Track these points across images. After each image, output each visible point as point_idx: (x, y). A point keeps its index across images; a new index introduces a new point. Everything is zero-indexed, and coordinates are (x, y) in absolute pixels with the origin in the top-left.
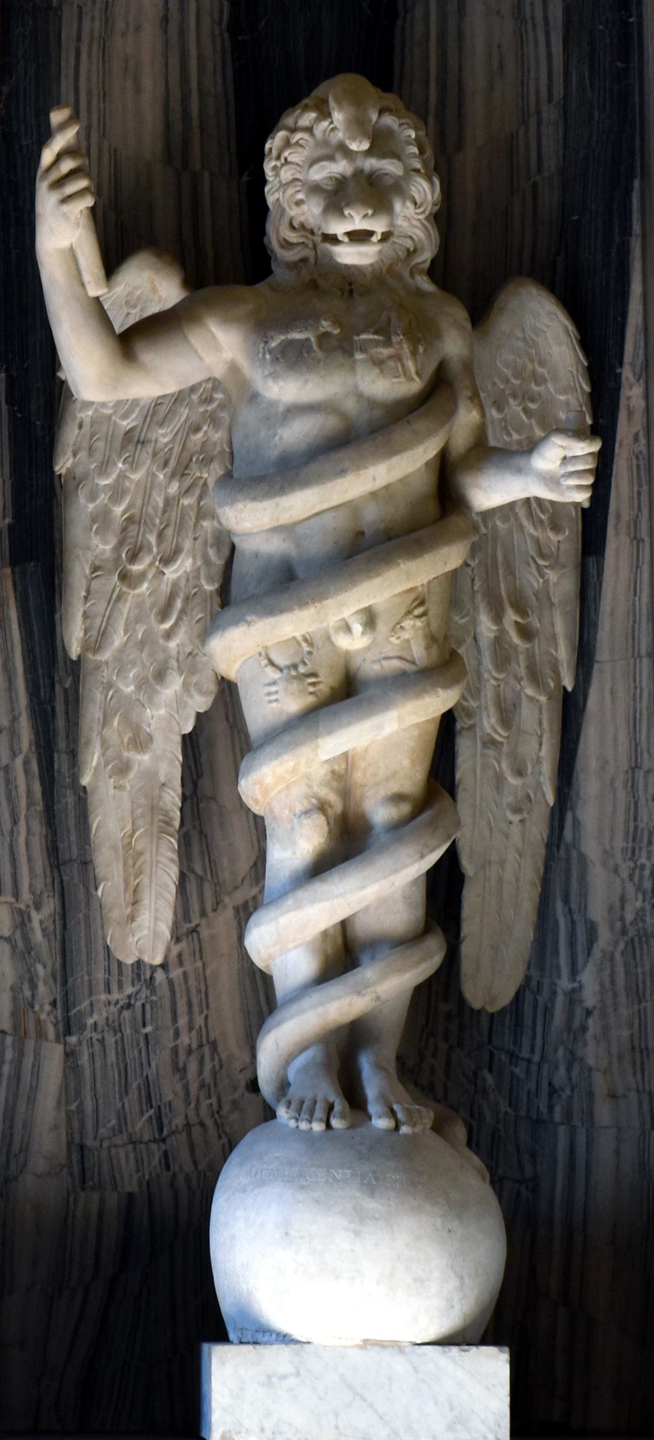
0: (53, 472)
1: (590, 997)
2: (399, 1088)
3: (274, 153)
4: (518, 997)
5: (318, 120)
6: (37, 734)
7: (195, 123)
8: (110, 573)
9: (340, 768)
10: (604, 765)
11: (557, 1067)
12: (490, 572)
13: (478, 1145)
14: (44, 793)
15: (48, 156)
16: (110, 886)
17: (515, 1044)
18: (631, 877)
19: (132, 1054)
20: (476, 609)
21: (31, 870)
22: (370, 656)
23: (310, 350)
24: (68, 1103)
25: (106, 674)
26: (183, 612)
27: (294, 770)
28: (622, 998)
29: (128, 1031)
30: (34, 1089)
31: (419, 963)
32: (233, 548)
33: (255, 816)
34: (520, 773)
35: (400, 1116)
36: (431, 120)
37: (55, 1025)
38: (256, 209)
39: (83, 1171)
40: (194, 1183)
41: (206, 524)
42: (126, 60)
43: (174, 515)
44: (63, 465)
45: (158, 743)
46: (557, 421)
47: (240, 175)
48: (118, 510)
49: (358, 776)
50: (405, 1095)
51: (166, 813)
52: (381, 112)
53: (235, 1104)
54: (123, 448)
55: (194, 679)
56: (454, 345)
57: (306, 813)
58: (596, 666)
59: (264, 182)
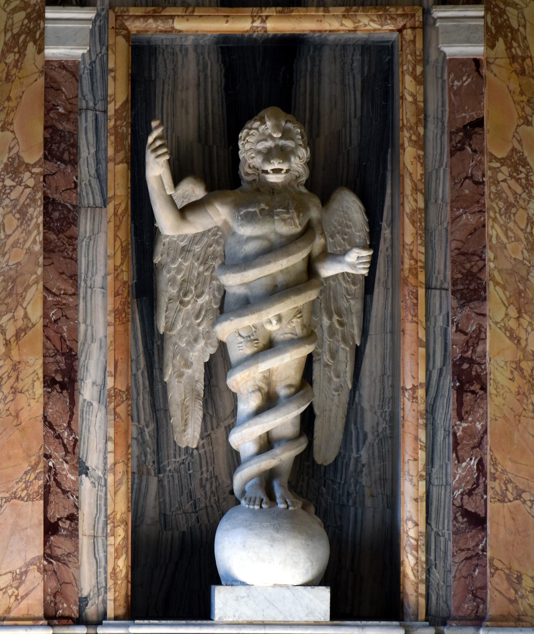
0: (153, 262)
1: (364, 459)
2: (289, 493)
3: (243, 138)
4: (336, 460)
5: (260, 125)
6: (147, 362)
7: (211, 126)
8: (176, 301)
9: (267, 375)
10: (371, 373)
11: (350, 485)
12: (327, 301)
13: (319, 514)
14: (149, 384)
15: (150, 139)
16: (176, 419)
17: (334, 477)
18: (381, 415)
19: (184, 481)
20: (322, 315)
21: (145, 413)
22: (279, 333)
23: (256, 215)
24: (159, 499)
25: (174, 339)
26: (205, 316)
27: (249, 376)
28: (377, 460)
29: (183, 472)
30: (146, 493)
31: (297, 447)
32: (225, 291)
33: (233, 393)
34: (338, 377)
35: (289, 503)
36: (307, 125)
37: (154, 470)
38: (235, 160)
39: (165, 523)
40: (209, 528)
41: (214, 282)
42: (183, 101)
43: (201, 279)
44: (157, 260)
45: (195, 365)
46: (356, 243)
47: (229, 147)
48: (179, 277)
49: (274, 378)
50: (291, 496)
51: (198, 392)
52: (286, 122)
53: (225, 499)
54: (181, 253)
55: (209, 341)
56: (314, 213)
57: (253, 392)
58: (369, 337)
59: (238, 149)
